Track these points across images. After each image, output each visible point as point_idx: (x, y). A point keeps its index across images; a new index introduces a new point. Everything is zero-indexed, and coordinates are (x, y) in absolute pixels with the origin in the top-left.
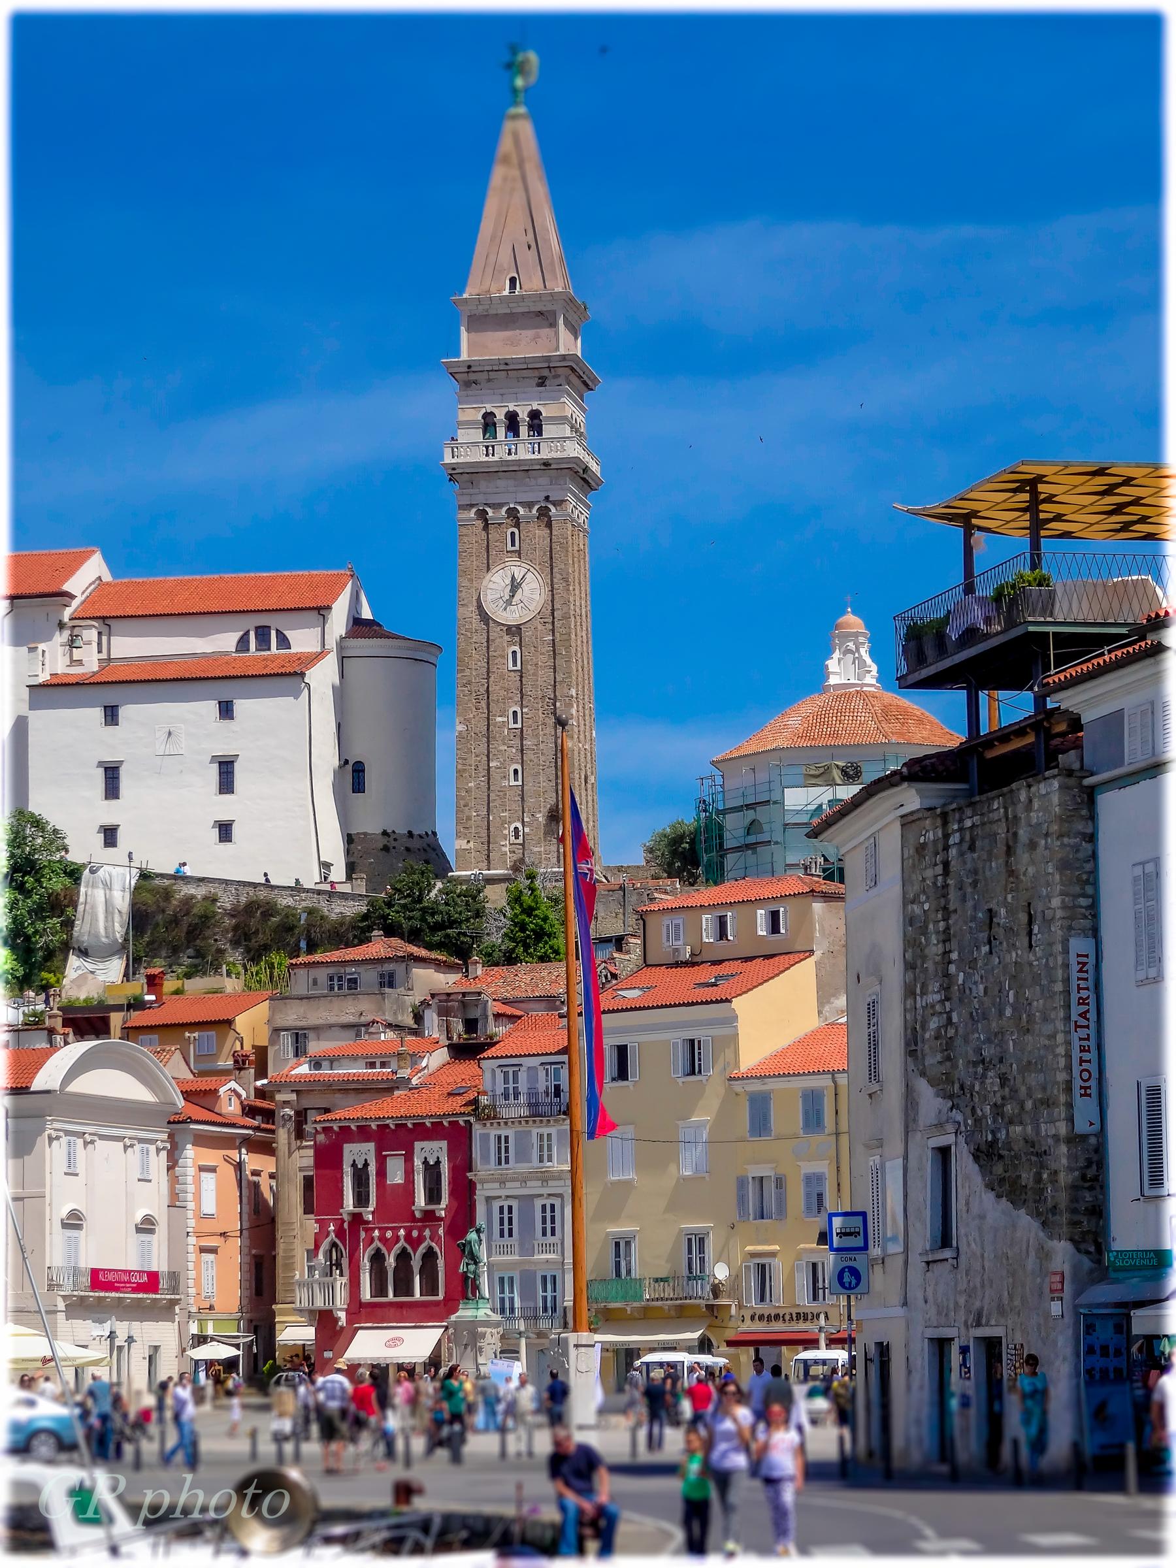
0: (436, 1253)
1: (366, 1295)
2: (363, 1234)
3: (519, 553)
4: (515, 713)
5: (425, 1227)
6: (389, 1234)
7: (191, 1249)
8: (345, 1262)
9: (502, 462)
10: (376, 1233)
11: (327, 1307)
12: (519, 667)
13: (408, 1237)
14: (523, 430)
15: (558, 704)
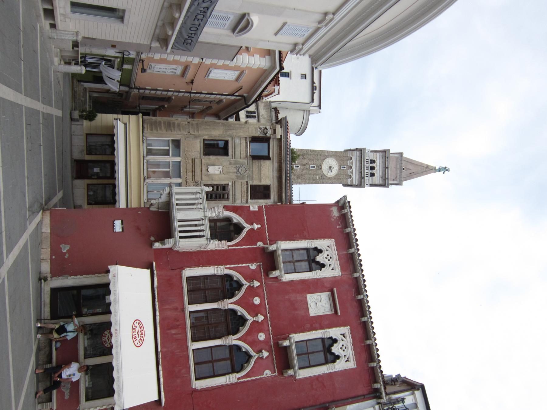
0: (241, 369)
1: (190, 272)
2: (253, 267)
3: (340, 169)
4: (298, 167)
5: (269, 351)
6: (257, 301)
7: (190, 59)
8: (223, 245)
9: (364, 165)
10: (256, 284)
11: (177, 229)
12: (311, 168)
13: (257, 327)
14: (371, 171)
15: (300, 180)
